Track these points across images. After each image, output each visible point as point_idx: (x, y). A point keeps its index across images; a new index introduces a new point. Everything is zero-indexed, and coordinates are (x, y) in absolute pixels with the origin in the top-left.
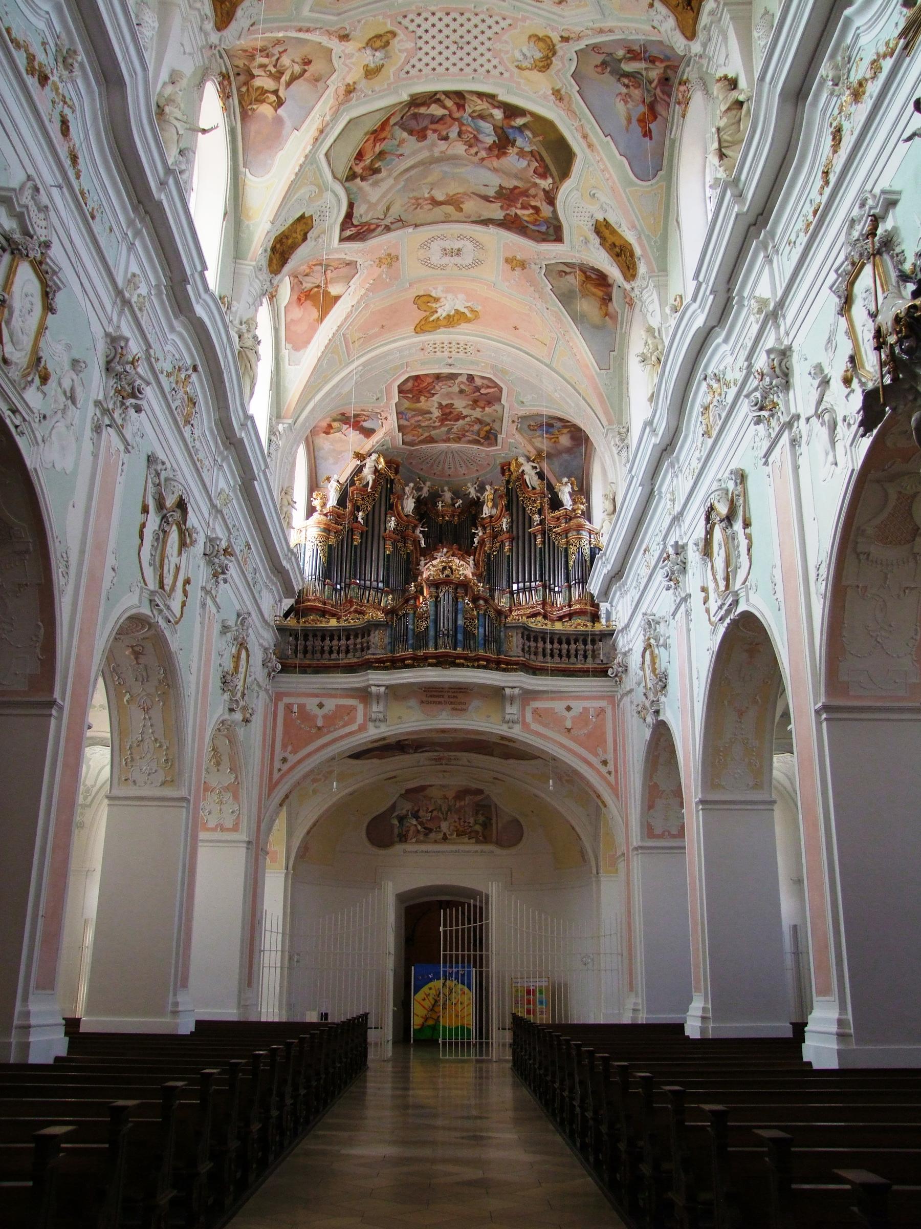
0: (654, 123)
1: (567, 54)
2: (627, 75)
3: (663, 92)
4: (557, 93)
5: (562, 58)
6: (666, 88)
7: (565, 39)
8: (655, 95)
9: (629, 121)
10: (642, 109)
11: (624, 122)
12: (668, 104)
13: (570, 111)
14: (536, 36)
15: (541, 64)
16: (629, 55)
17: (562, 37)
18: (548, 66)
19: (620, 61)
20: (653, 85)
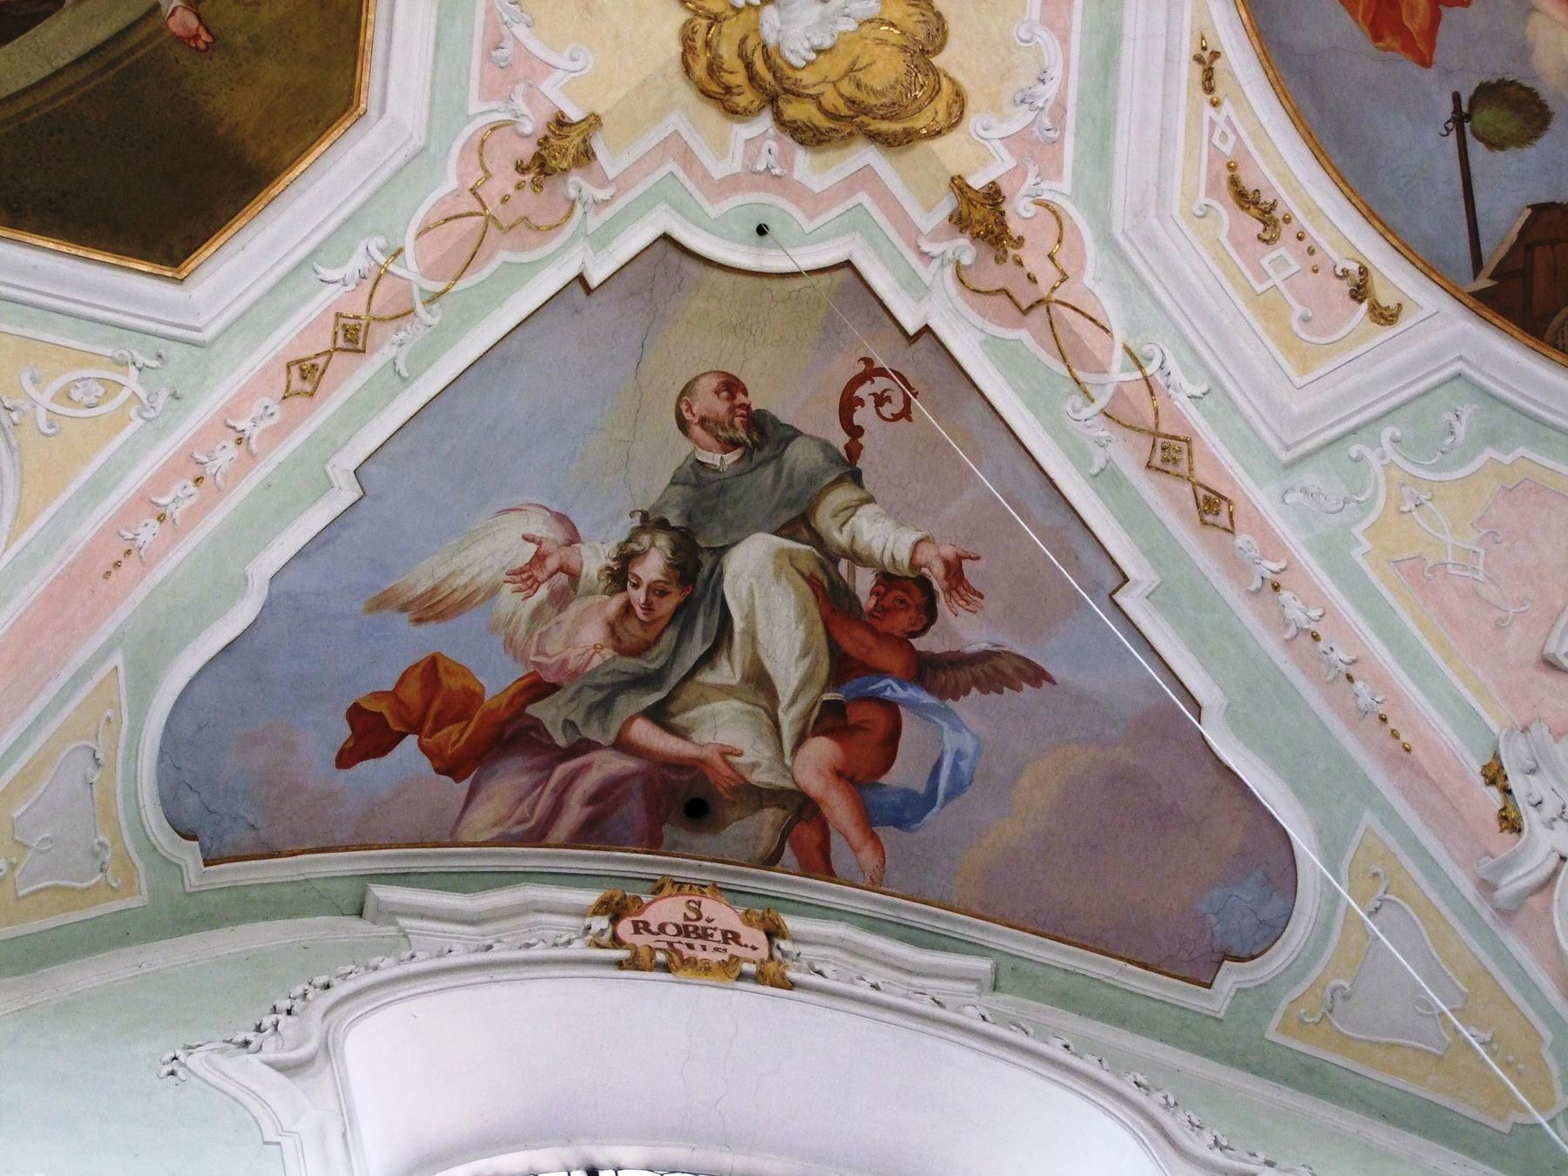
0: (425, 765)
1: (858, 218)
2: (695, 571)
3: (606, 796)
4: (559, 152)
5: (777, 181)
6: (634, 809)
7: (982, 216)
8: (584, 747)
9: (432, 608)
10: (496, 678)
11: (420, 579)
12: (536, 836)
13: (478, 231)
14: (938, 33)
15: (728, 52)
16: (864, 583)
17: (994, 195)
18: (720, 97)
19: (800, 525)
20: (645, 733)
